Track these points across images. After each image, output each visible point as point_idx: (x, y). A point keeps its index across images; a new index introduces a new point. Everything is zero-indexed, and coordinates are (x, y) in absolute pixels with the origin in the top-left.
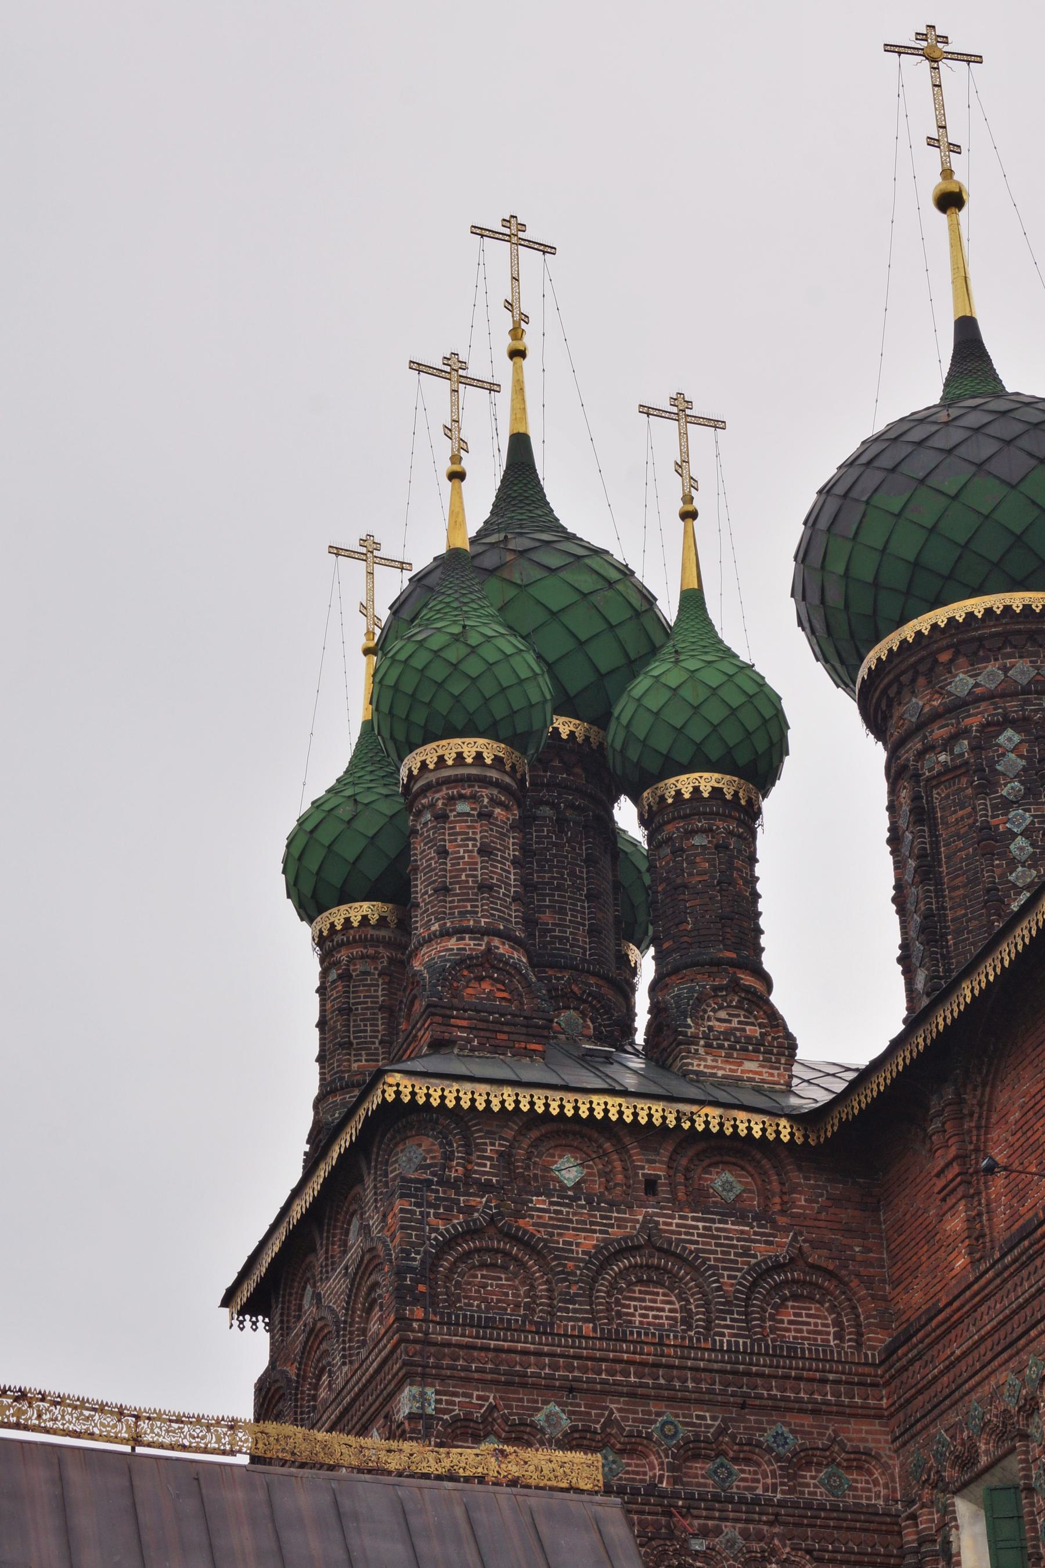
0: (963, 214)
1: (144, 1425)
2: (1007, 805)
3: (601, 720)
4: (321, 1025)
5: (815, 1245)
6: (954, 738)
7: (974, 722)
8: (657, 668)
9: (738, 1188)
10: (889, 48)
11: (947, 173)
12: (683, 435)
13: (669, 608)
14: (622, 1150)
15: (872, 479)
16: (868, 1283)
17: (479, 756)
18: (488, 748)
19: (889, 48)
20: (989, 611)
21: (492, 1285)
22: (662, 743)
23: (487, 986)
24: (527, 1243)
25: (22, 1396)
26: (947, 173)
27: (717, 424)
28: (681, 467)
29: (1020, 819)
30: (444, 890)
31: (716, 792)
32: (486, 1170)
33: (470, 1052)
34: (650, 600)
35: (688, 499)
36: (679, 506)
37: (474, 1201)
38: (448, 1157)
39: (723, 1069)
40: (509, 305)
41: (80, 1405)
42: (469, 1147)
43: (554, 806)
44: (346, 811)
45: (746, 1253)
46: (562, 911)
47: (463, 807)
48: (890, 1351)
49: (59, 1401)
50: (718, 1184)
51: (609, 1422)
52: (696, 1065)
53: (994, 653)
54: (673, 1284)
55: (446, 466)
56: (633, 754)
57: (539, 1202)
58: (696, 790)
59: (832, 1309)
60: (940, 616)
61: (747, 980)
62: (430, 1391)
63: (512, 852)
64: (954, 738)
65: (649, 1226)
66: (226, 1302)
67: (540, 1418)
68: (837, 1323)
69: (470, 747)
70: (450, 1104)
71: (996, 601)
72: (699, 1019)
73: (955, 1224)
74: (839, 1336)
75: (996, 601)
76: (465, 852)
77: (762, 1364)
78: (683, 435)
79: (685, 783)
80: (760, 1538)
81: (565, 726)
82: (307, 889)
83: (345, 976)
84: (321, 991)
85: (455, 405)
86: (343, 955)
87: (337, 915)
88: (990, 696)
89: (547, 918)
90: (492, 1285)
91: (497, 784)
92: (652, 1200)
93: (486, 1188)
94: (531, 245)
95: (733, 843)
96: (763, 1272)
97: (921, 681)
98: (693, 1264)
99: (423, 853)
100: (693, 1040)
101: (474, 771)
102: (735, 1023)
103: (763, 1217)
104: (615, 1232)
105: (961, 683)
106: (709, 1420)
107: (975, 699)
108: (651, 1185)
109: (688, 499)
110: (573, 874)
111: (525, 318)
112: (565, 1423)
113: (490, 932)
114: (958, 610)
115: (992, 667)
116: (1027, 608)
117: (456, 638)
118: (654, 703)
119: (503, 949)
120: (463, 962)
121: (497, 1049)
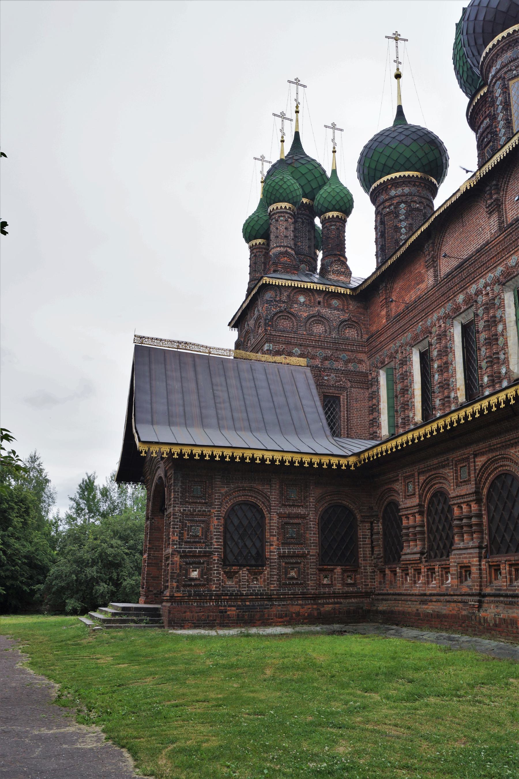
0: (401, 80)
1: (211, 350)
2: (401, 221)
3: (313, 199)
4: (250, 266)
5: (353, 316)
6: (390, 205)
7: (395, 202)
8: (325, 187)
9: (338, 304)
10: (386, 37)
11: (398, 69)
12: (334, 132)
13: (329, 174)
14: (313, 295)
15: (376, 144)
16: (364, 325)
17: (286, 207)
18: (288, 205)
19: (386, 37)
20: (400, 176)
21: (285, 323)
22: (326, 205)
23: (286, 259)
24: (293, 315)
25: (186, 343)
26: (398, 69)
27: (341, 130)
28: (333, 140)
29: (404, 224)
30: (277, 237)
31: (337, 216)
32: (284, 298)
33: (282, 273)
34: (324, 172)
35: (334, 148)
36: (332, 149)
37: (281, 305)
38: (276, 296)
39: (336, 278)
40: (296, 100)
41: (198, 345)
42: (281, 294)
43: (302, 219)
44: (256, 219)
45: (339, 318)
46: (303, 242)
47: (282, 218)
48: (368, 339)
49: (194, 344)
50: (333, 303)
51: (308, 352)
52: (330, 277)
53: (401, 186)
54: (323, 324)
55: (280, 139)
56: (319, 207)
57: (295, 306)
58: (333, 216)
59: (356, 330)
60: (389, 177)
61: (342, 259)
62: (271, 345)
63: (292, 229)
64: (390, 205)
65: (318, 311)
66: (229, 325)
67: (294, 351)
68: (357, 333)
69: (283, 205)
70: (277, 284)
71: (402, 174)
72: (331, 267)
73: (384, 313)
74: (358, 336)
75: (402, 174)
76: (282, 229)
77: (341, 341)
78: (334, 132)
79: (330, 214)
80: (339, 377)
81: (305, 200)
82: (247, 236)
83: (255, 256)
84: (250, 259)
85: (283, 124)
86: (255, 251)
87: (254, 242)
88: (399, 196)
89: (299, 244)
90: (285, 323)
91: (289, 213)
93: (284, 302)
94: (301, 85)
95: (340, 228)
96: (342, 322)
97: (384, 192)
98: (327, 320)
99: (273, 229)
100: (330, 272)
101: (284, 210)
103: (343, 310)
104: (311, 313)
105: (393, 193)
106: (329, 353)
107: (396, 196)
108: (319, 303)
109: (334, 148)
110: (305, 234)
111: (299, 103)
112: (299, 352)
113: (286, 247)
114: (393, 176)
115: (400, 189)
116: (409, 175)
117: (281, 179)
118: (324, 196)
119: (289, 250)
120: (281, 253)
121: (287, 272)
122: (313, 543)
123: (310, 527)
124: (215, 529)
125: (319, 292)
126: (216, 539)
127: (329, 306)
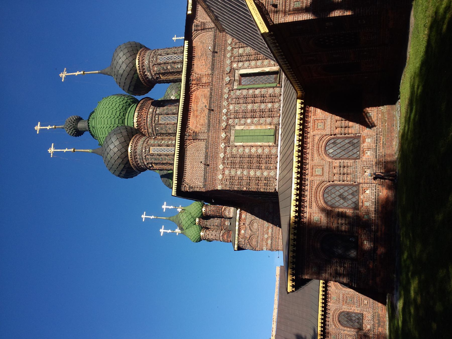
9: (244, 215)
23: (225, 236)
37: (246, 242)
43: (205, 222)
46: (216, 222)
47: (207, 236)
65: (248, 225)
74: (257, 207)
89: (216, 224)
92: (245, 224)
102: (227, 211)
104: (249, 228)
108: (244, 224)
110: (212, 221)
112: (266, 235)
119: (221, 235)
122: (354, 293)
123: (348, 293)
124: (348, 332)
125: (239, 224)
126: (352, 332)
127: (245, 219)
